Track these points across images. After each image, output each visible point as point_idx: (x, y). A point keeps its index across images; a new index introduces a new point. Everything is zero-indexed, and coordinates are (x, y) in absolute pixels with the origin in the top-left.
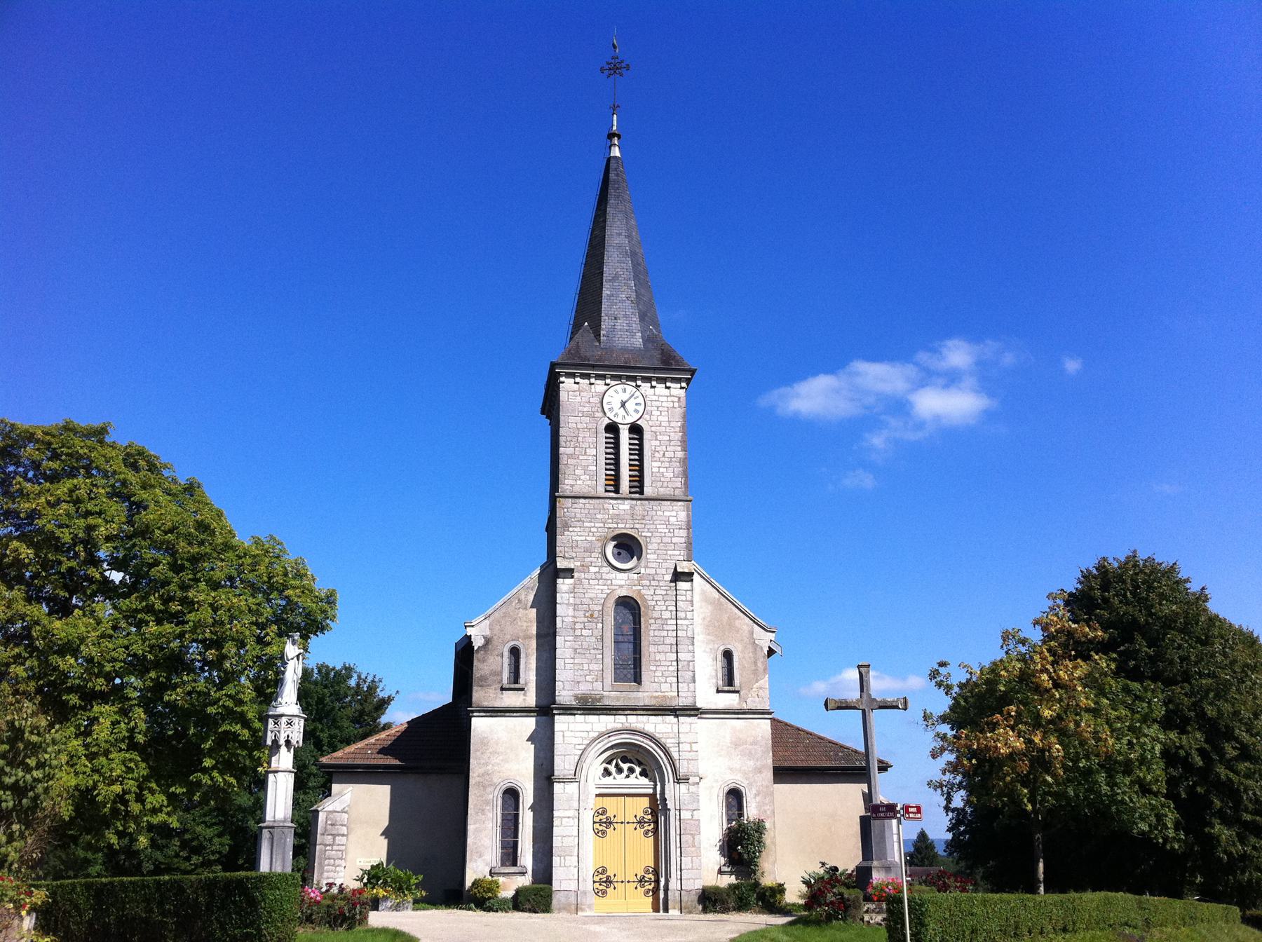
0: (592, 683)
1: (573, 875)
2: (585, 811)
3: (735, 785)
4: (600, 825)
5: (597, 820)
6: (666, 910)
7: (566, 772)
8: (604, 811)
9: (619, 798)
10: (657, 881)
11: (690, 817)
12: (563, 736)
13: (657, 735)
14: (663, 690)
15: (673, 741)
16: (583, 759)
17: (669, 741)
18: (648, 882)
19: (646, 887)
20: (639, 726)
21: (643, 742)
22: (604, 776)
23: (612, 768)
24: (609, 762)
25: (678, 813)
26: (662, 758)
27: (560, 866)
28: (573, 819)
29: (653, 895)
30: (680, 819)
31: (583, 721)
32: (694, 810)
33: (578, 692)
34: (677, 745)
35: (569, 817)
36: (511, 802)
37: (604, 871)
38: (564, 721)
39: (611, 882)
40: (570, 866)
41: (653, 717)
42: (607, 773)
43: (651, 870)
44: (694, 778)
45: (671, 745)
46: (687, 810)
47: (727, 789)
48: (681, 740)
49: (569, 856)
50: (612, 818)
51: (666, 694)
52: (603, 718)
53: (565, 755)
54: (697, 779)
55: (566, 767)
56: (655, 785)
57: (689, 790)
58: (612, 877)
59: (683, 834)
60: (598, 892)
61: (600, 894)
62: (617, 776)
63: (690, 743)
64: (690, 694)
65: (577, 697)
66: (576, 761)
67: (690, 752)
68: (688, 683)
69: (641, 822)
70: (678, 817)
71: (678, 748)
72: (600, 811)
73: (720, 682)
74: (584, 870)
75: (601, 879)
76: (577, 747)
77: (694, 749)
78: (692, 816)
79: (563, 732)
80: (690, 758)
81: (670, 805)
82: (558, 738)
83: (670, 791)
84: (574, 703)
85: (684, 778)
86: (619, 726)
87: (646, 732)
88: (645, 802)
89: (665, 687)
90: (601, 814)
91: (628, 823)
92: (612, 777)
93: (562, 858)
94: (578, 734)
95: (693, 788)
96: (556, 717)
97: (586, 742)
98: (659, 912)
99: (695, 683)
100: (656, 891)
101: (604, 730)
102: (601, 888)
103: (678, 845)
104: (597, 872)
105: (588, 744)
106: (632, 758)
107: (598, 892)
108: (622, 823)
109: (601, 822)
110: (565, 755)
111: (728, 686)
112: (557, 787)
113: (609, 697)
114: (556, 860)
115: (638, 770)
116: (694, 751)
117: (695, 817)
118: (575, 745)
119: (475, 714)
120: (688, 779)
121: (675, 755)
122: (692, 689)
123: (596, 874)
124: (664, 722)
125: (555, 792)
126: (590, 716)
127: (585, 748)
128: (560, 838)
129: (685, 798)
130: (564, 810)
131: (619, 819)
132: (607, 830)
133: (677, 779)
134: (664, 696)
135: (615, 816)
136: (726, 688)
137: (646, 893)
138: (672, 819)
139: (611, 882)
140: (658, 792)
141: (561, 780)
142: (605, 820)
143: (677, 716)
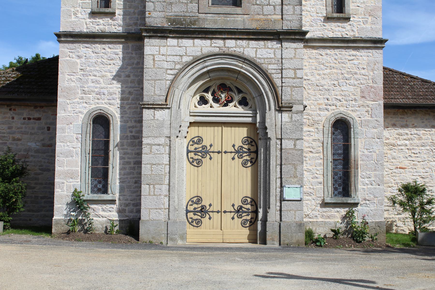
0: (187, 4)
1: (164, 204)
2: (177, 139)
3: (341, 115)
4: (195, 154)
5: (192, 148)
6: (264, 242)
7: (157, 98)
8: (200, 140)
9: (216, 128)
10: (256, 212)
11: (293, 147)
12: (154, 60)
13: (258, 60)
14: (265, 13)
15: (275, 67)
16: (176, 84)
17: (270, 67)
18: (246, 212)
19: (245, 218)
20: (239, 51)
21: (242, 68)
22: (199, 103)
23: (209, 96)
24: (206, 91)
25: (279, 142)
26: (262, 85)
27: (150, 195)
28: (163, 147)
29: (250, 226)
30: (281, 149)
31: (176, 44)
32: (297, 139)
33: (170, 14)
34: (280, 71)
35: (159, 145)
36: (101, 129)
37: (199, 200)
38: (154, 44)
39: (207, 212)
40: (160, 195)
41: (253, 42)
42: (203, 101)
43: (249, 200)
44: (297, 106)
45: (273, 71)
46: (289, 139)
47: (333, 120)
48: (285, 66)
49: (158, 184)
50: (209, 147)
51: (269, 17)
52: (198, 42)
53: (155, 80)
54: (301, 108)
55: (156, 92)
56: (255, 117)
57: (292, 118)
58: (208, 207)
59: (285, 164)
60: (192, 222)
61: (194, 224)
62: (214, 105)
63: (295, 69)
64: (295, 17)
65: (169, 20)
66: (167, 86)
67: (294, 78)
68: (294, 6)
69: (239, 152)
70: (279, 147)
71: (280, 76)
72: (195, 140)
73: (330, 9)
74: (176, 199)
75: (195, 209)
76: (169, 72)
77: (299, 75)
78: (295, 145)
79: (153, 55)
80: (294, 85)
81: (271, 133)
82: (148, 62)
83: (271, 120)
84: (166, 25)
85: (287, 105)
86: (217, 50)
87: (245, 57)
88: (243, 132)
89: (268, 9)
90: (196, 143)
91: (225, 152)
92: (208, 105)
93: (152, 186)
94: (169, 59)
95: (296, 117)
96: (146, 40)
97: (178, 67)
98: (256, 243)
99: (301, 4)
100: (253, 222)
101: (199, 54)
102: (196, 217)
103: (279, 176)
104: (191, 201)
105: (181, 69)
106: (231, 86)
107: (192, 222)
108: (219, 152)
109: (196, 152)
110: (155, 80)
111: (338, 12)
112: (147, 114)
113: (204, 20)
114: (145, 188)
115: (237, 97)
116: (298, 78)
117: (298, 147)
118: (167, 69)
119: (62, 39)
120: (292, 107)
121: (278, 82)
122: (298, 12)
123: (190, 203)
124: (266, 47)
125: (144, 119)
126: (184, 40)
127: (178, 73)
128: (149, 166)
129: (288, 126)
130: (154, 137)
131: (216, 148)
132: (203, 159)
133: (279, 107)
134: (267, 20)
135: (211, 146)
136: (335, 15)
137: (243, 224)
138: (273, 149)
139: (207, 212)
140: (258, 120)
141: (151, 106)
142: (201, 149)
143: (280, 41)
